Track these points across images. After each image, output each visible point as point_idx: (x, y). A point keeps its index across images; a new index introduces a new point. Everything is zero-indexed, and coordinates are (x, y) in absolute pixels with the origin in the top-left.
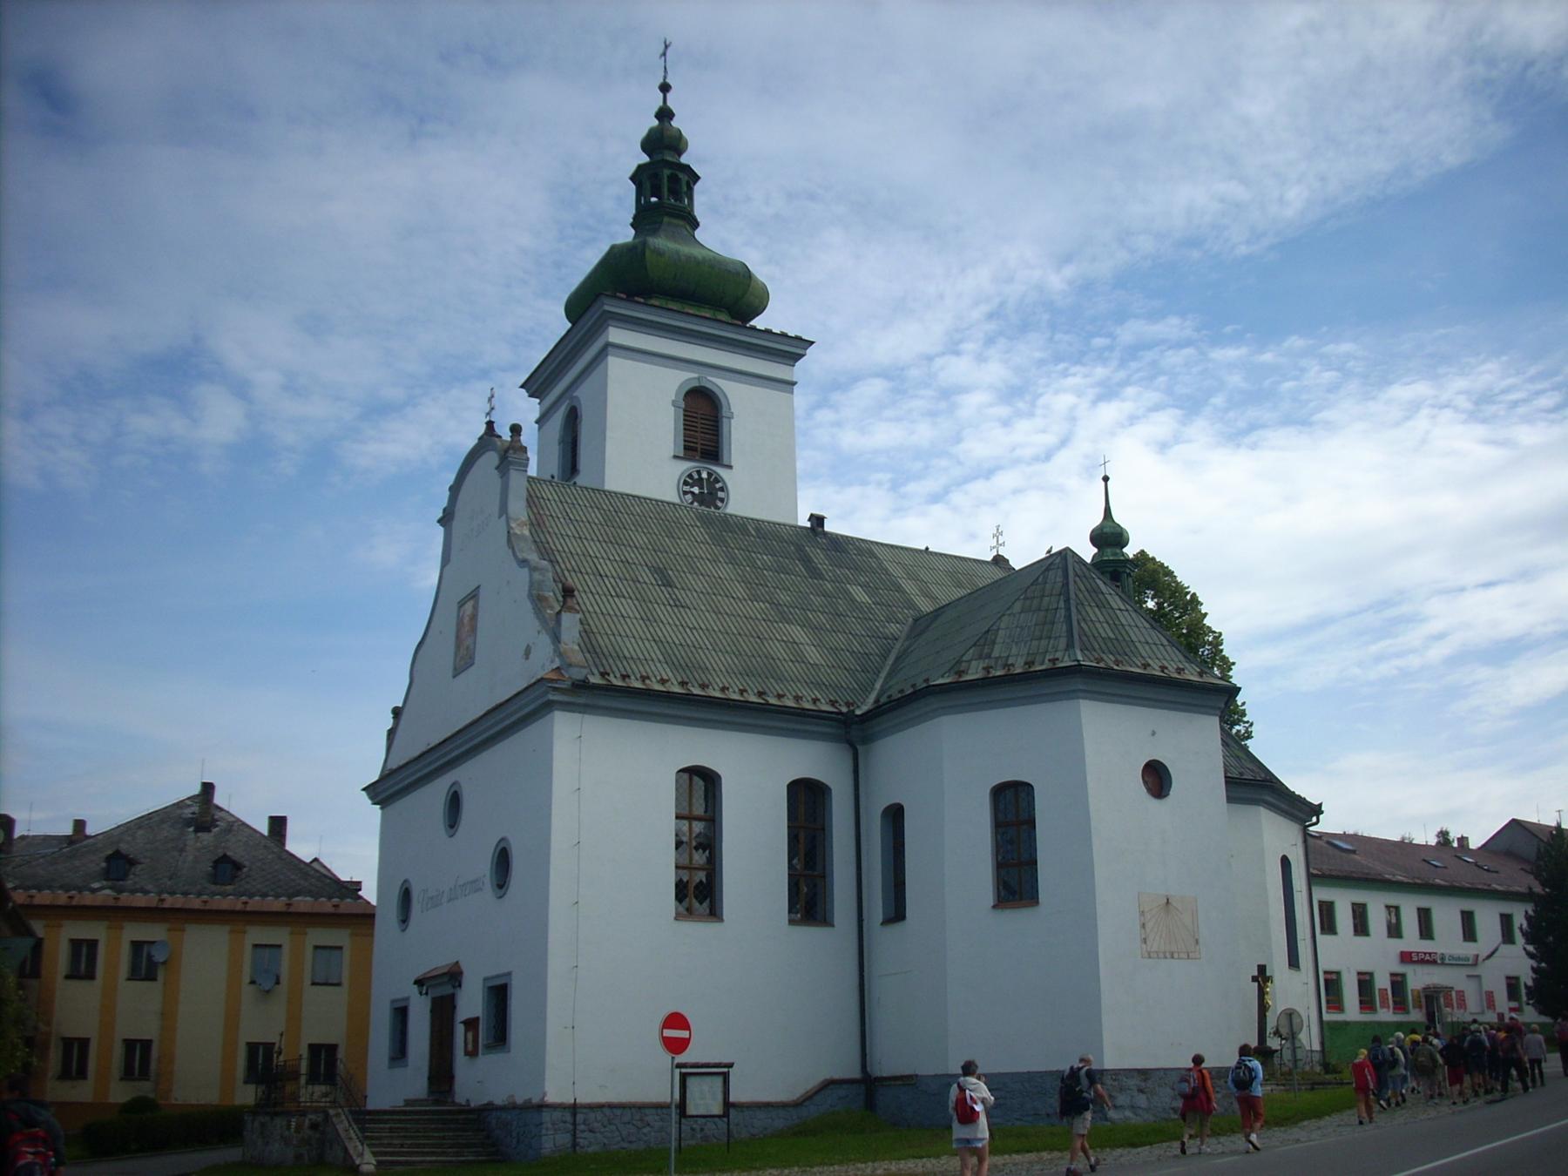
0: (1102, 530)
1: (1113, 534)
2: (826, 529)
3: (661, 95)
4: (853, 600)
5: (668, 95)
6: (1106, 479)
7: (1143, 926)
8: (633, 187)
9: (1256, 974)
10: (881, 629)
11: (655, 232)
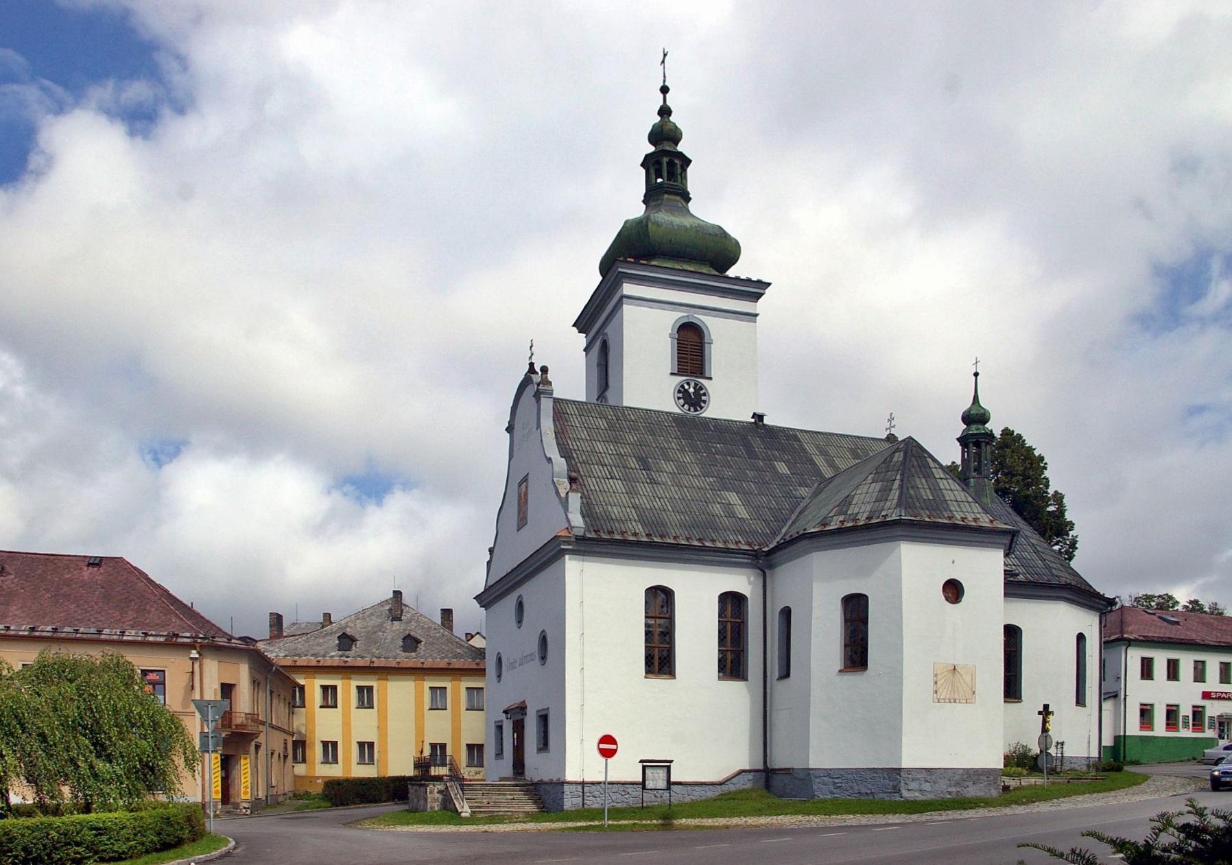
2: (765, 422)
3: (662, 96)
4: (777, 472)
5: (667, 95)
8: (643, 171)
9: (1042, 710)
10: (794, 492)
11: (658, 208)
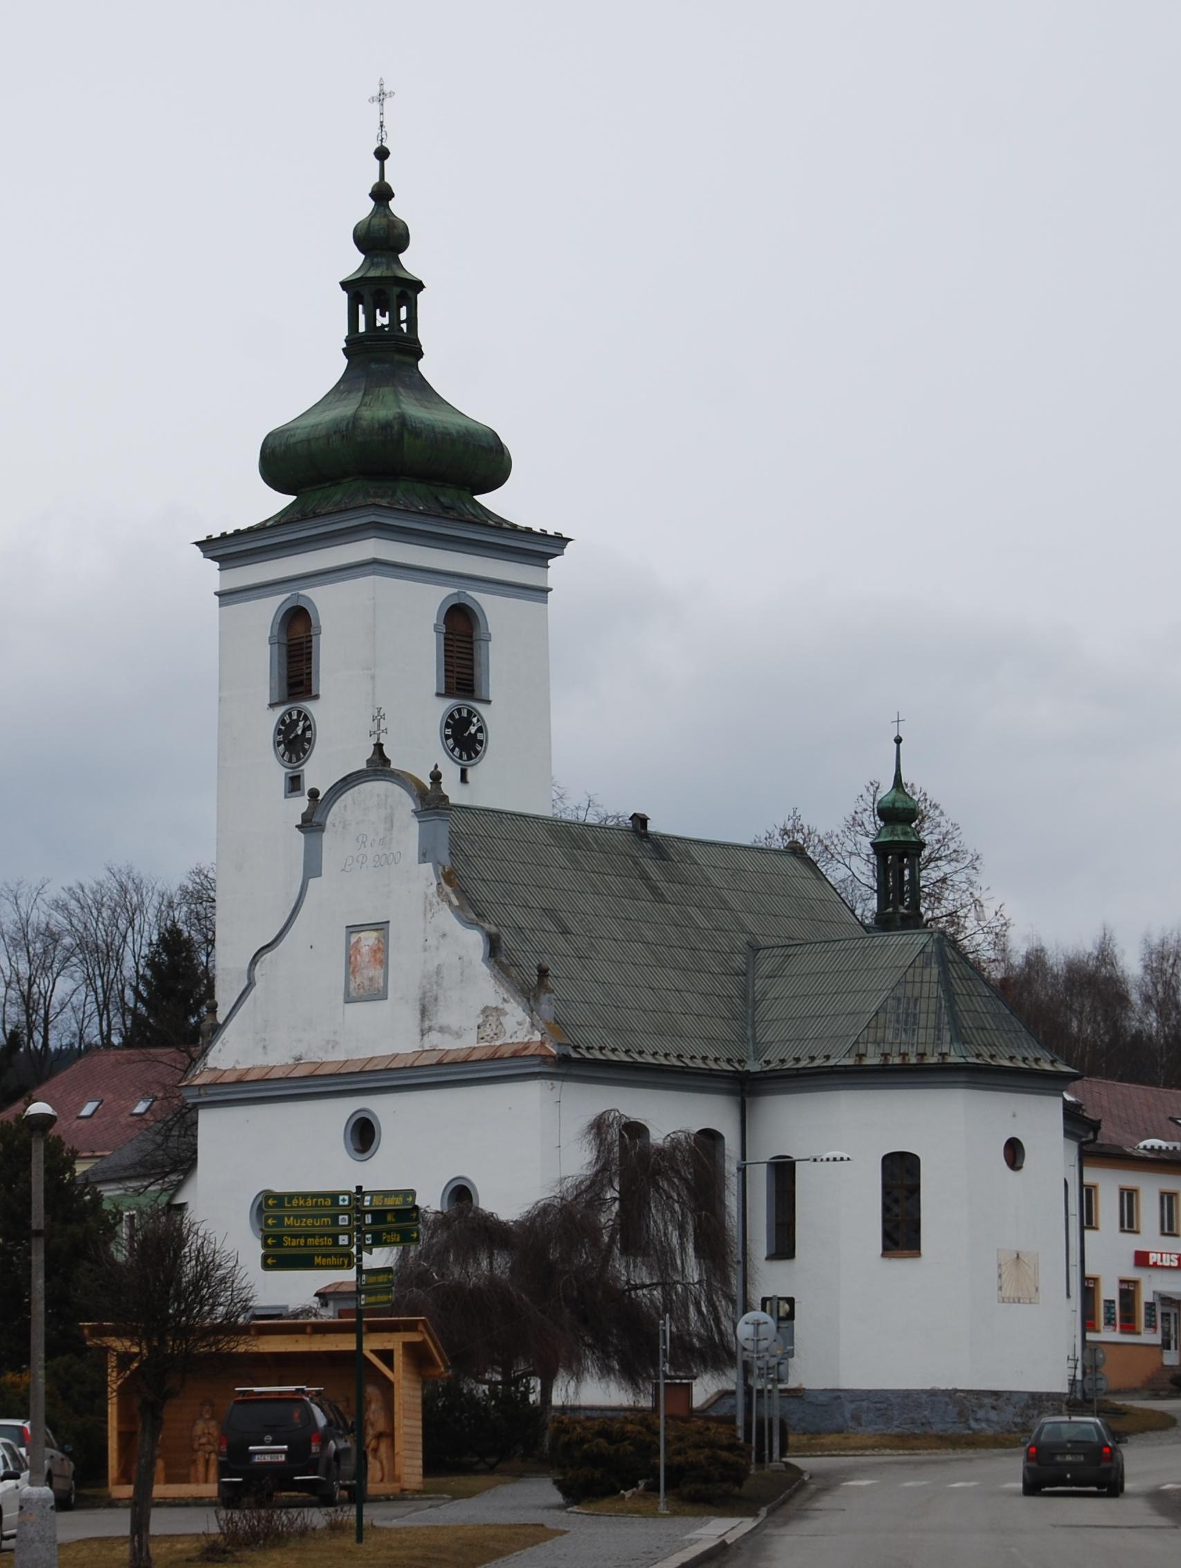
0: (894, 804)
1: (904, 809)
6: (898, 741)
7: (1000, 1276)
